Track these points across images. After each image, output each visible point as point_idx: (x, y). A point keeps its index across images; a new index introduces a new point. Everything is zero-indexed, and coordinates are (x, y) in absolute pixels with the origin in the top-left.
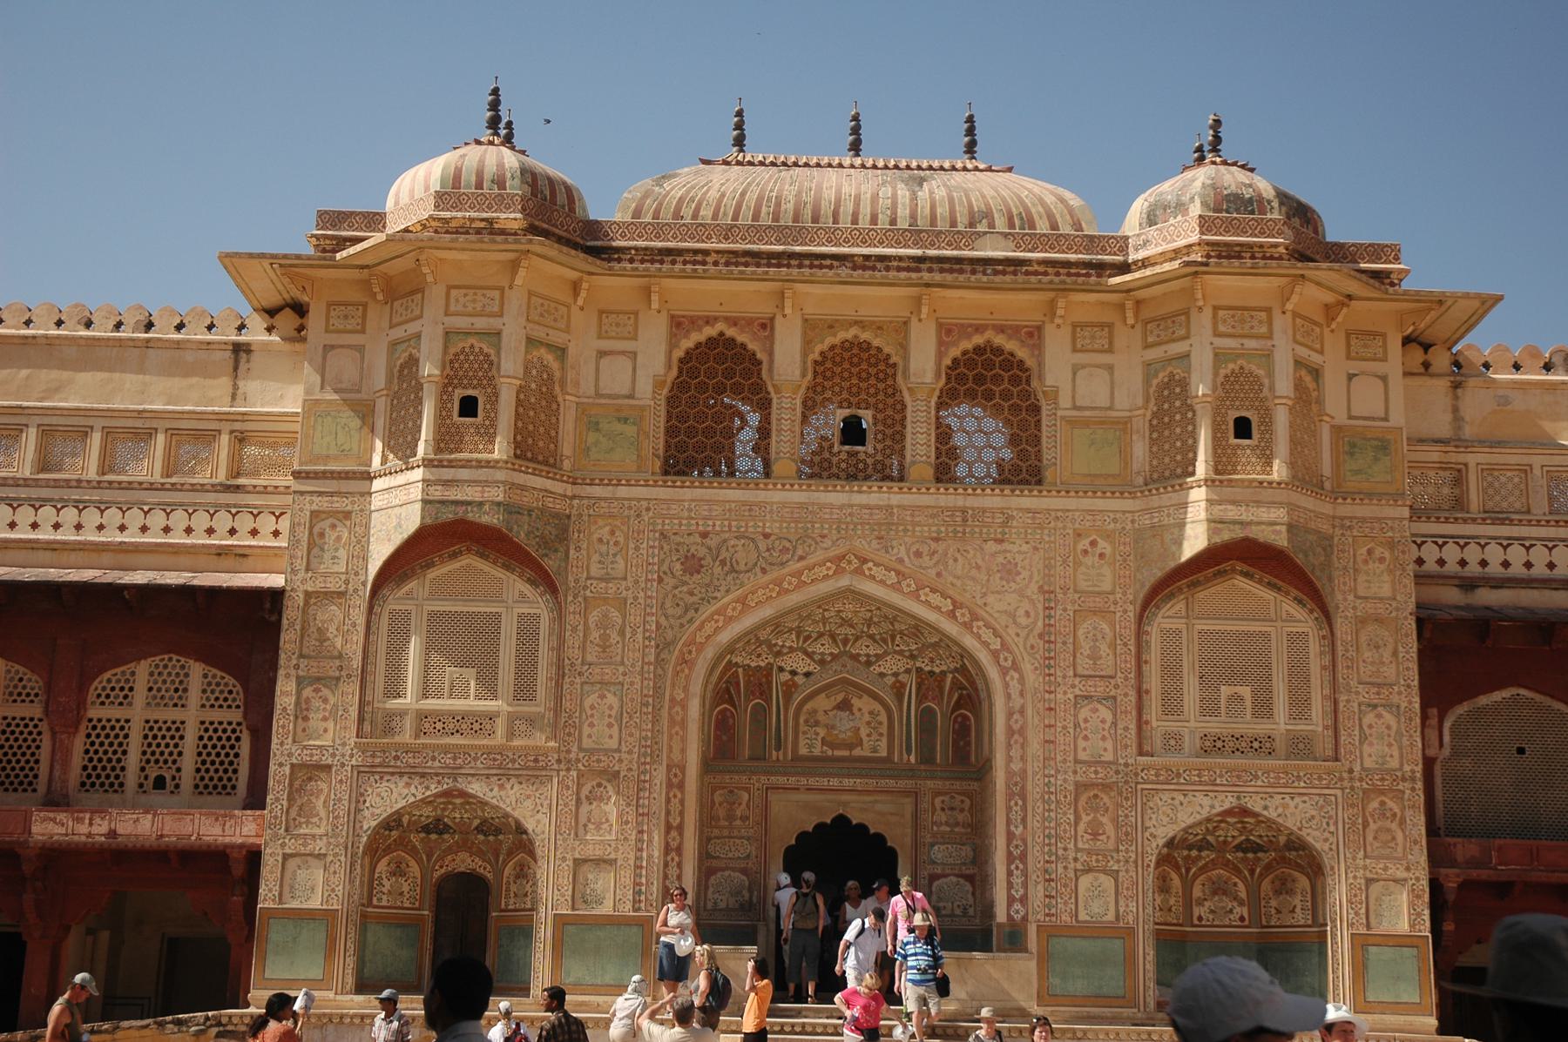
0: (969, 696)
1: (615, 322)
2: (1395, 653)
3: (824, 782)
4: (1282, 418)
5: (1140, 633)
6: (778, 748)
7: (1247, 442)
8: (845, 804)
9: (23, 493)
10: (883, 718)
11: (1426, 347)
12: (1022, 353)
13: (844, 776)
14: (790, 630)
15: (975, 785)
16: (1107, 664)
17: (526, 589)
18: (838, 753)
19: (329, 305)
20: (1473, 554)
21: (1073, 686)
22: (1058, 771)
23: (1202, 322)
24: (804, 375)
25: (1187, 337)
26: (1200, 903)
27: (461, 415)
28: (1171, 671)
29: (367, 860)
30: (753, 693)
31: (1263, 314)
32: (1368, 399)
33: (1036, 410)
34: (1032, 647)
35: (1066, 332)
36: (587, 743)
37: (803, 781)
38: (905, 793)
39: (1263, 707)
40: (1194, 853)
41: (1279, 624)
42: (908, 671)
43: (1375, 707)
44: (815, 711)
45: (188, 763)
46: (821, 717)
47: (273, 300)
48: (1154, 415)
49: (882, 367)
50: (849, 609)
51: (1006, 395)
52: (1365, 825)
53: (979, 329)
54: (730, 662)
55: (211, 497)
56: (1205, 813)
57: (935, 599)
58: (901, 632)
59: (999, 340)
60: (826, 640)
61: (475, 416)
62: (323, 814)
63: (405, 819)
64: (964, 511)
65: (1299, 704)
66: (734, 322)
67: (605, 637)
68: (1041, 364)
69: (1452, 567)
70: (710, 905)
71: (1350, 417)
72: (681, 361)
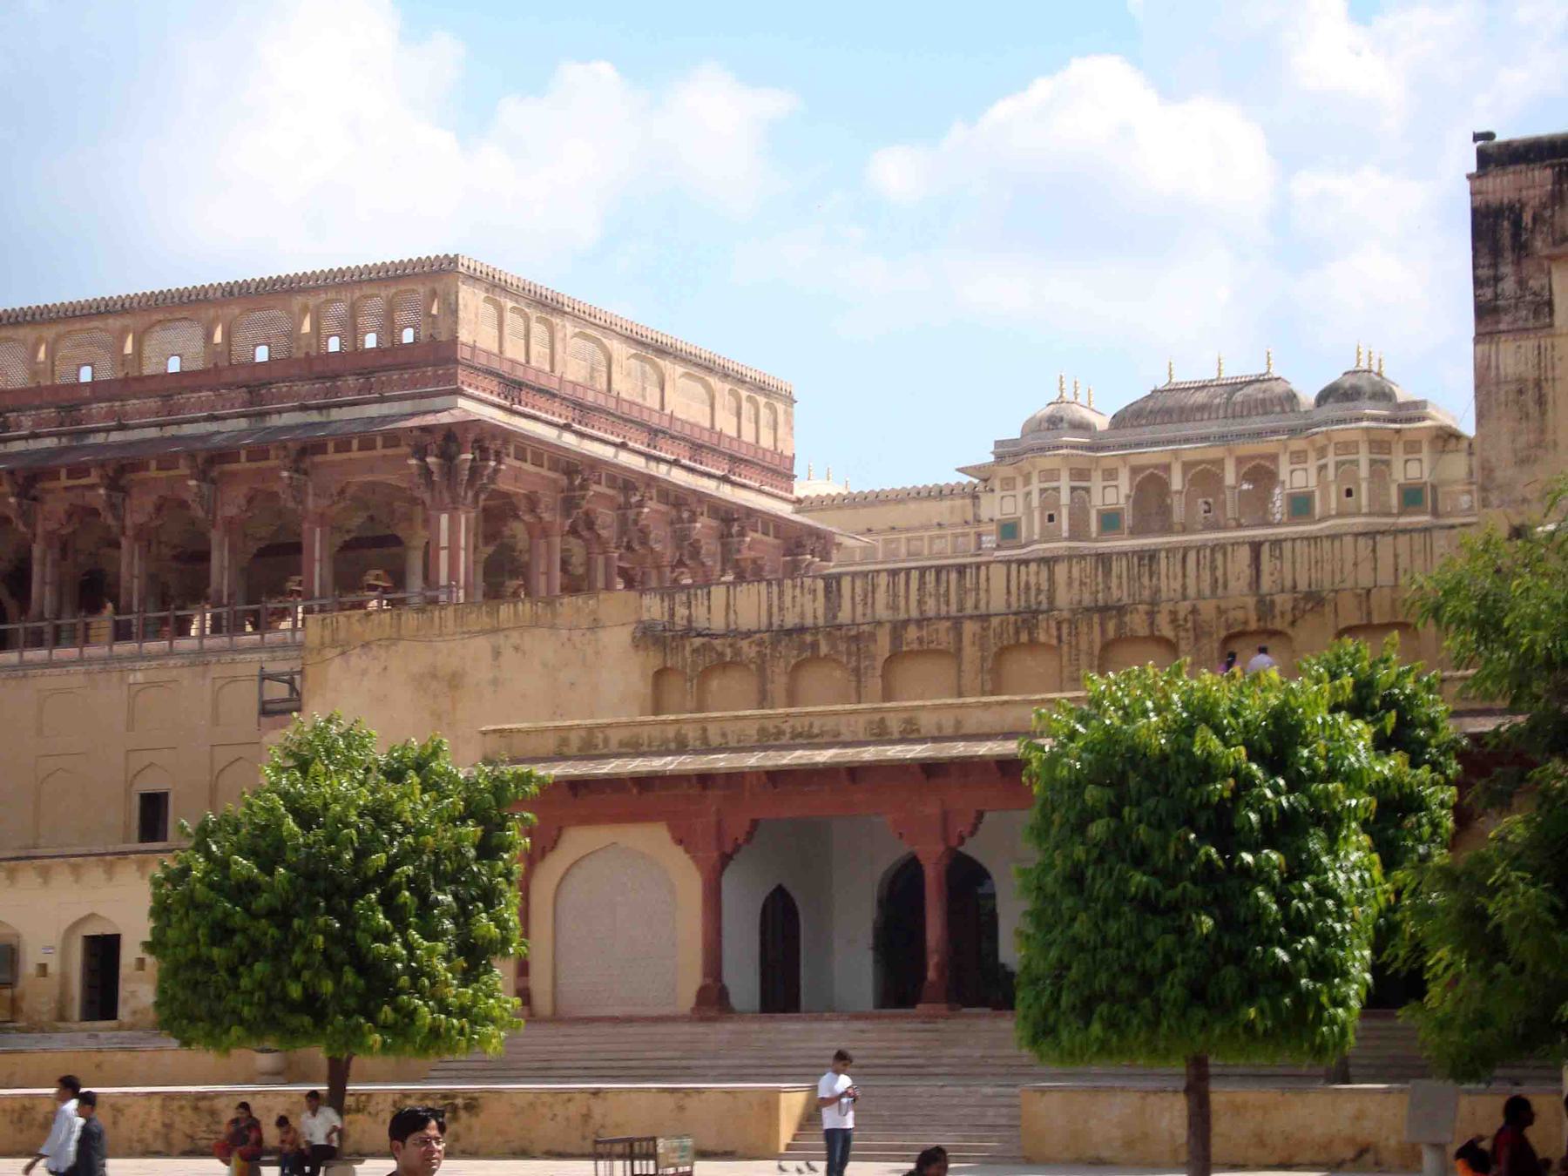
1: (1110, 474)
4: (1364, 486)
23: (1331, 449)
32: (1414, 471)
53: (1252, 458)
66: (1156, 467)
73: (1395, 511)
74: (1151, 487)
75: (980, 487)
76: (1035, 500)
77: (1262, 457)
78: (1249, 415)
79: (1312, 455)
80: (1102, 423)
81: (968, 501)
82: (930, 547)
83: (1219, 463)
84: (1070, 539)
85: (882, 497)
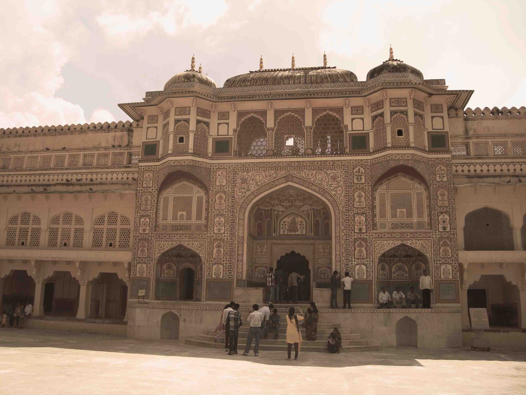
1: (224, 116)
2: (448, 197)
5: (372, 195)
7: (401, 137)
9: (79, 171)
10: (304, 223)
11: (456, 109)
12: (337, 116)
14: (275, 199)
16: (364, 205)
17: (200, 190)
18: (291, 233)
19: (149, 116)
20: (472, 168)
23: (387, 103)
24: (275, 125)
25: (383, 108)
26: (394, 273)
27: (180, 142)
28: (383, 205)
29: (159, 265)
31: (404, 100)
32: (438, 124)
33: (342, 132)
35: (350, 108)
36: (216, 231)
37: (281, 242)
38: (311, 244)
39: (410, 214)
40: (392, 258)
41: (414, 190)
42: (310, 210)
43: (442, 213)
45: (117, 239)
46: (286, 223)
47: (138, 118)
48: (375, 131)
49: (297, 122)
50: (291, 191)
51: (333, 128)
52: (440, 248)
53: (324, 109)
55: (122, 170)
56: (393, 246)
57: (314, 187)
59: (331, 113)
61: (183, 142)
62: (146, 252)
63: (170, 254)
64: (321, 161)
65: (420, 214)
66: (256, 112)
68: (343, 119)
69: (466, 172)
70: (256, 277)
71: (433, 129)
72: (241, 125)
73: (427, 149)
74: (251, 126)
75: (134, 125)
76: (171, 127)
77: (331, 109)
78: (322, 82)
79: (367, 110)
80: (220, 84)
81: (125, 133)
82: (98, 160)
83: (301, 112)
84: (194, 154)
85: (72, 129)
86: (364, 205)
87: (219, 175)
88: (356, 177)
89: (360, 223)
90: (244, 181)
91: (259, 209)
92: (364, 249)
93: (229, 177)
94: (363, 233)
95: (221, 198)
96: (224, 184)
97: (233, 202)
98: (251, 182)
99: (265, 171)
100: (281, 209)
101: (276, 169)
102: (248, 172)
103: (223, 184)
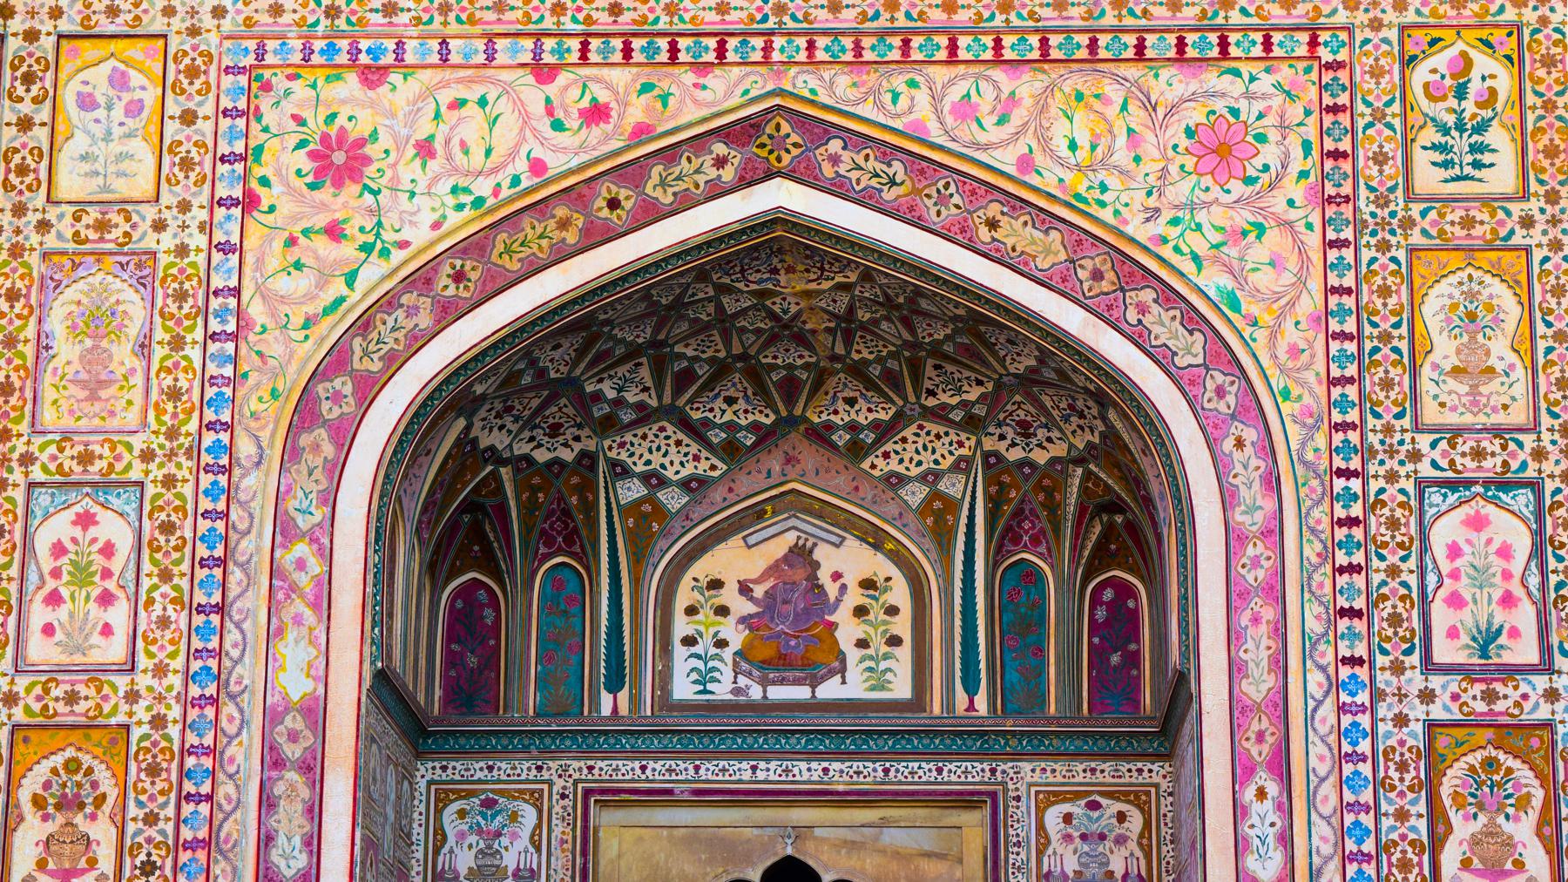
0: (1132, 527)
3: (741, 772)
6: (614, 688)
8: (801, 832)
10: (900, 594)
13: (795, 754)
14: (633, 353)
15: (1156, 773)
16: (1510, 397)
18: (778, 693)
21: (1415, 456)
22: (1377, 695)
30: (548, 545)
34: (1294, 352)
36: (39, 650)
38: (965, 800)
44: (716, 584)
54: (466, 443)
57: (1017, 233)
58: (936, 350)
60: (736, 384)
67: (94, 357)
86: (1510, 397)
87: (87, 102)
88: (1430, 135)
89: (1481, 576)
90: (338, 161)
91: (468, 453)
92: (1523, 830)
93: (188, 118)
94: (1511, 672)
95: (97, 324)
96: (143, 184)
97: (222, 360)
98: (410, 170)
99: (543, 73)
100: (678, 459)
101: (651, 50)
102: (373, 75)
103: (122, 188)
